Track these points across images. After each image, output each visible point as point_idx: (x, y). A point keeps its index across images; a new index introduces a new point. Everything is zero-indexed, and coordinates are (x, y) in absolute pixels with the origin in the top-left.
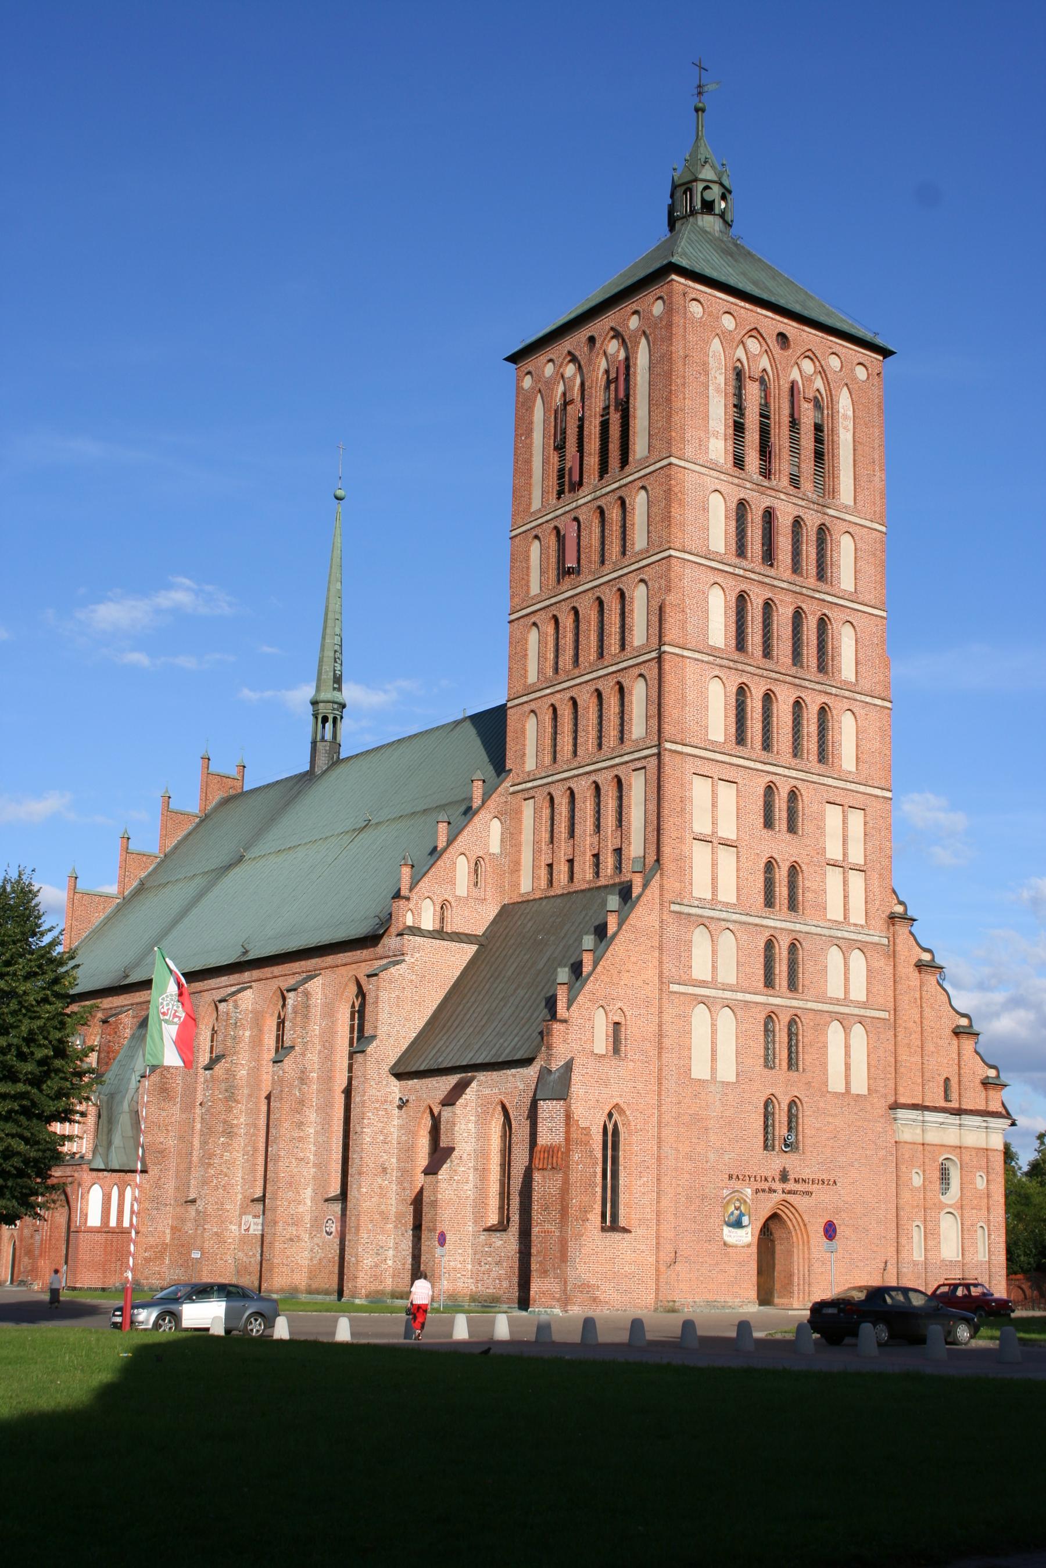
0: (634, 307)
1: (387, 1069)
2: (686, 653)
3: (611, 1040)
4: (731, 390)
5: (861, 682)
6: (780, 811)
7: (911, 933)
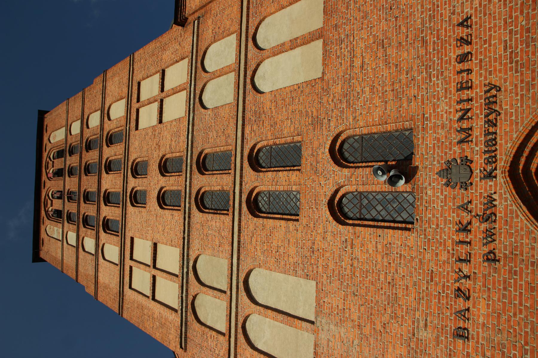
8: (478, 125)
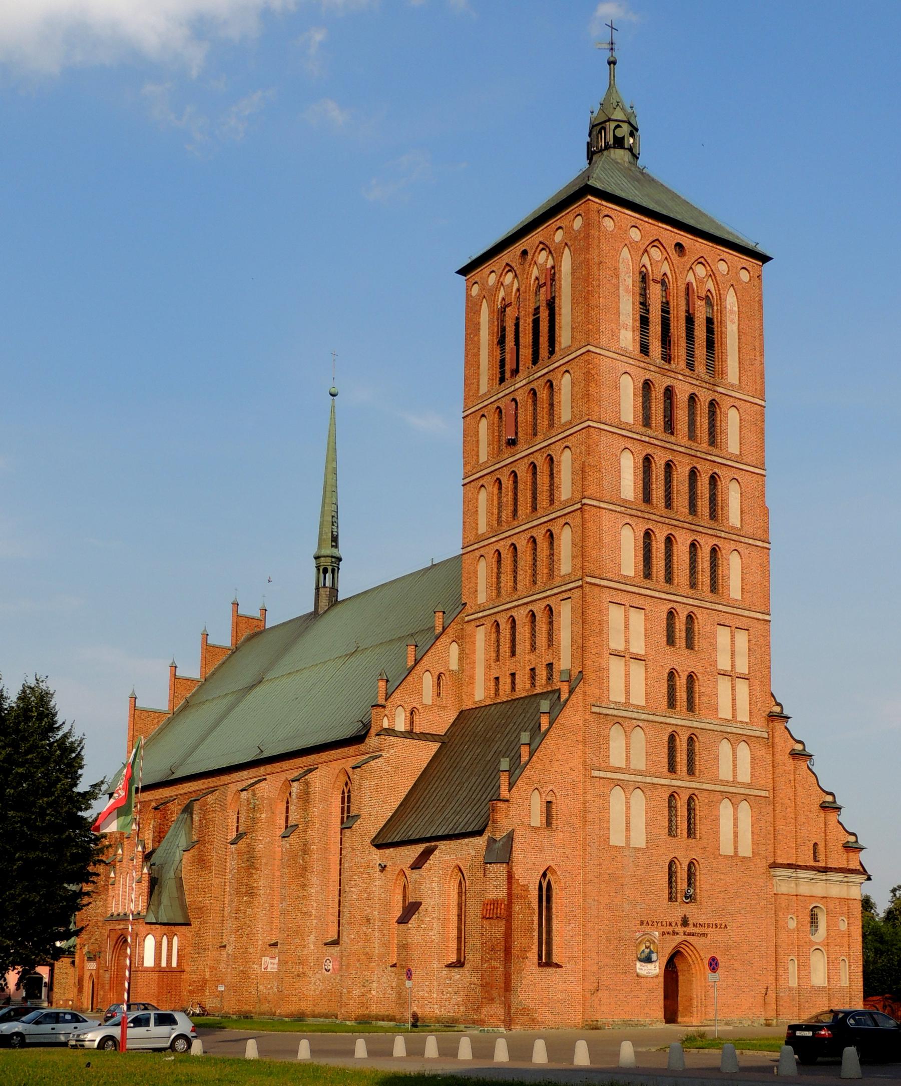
0: (559, 224)
1: (369, 841)
2: (602, 505)
3: (544, 815)
4: (637, 290)
5: (746, 528)
6: (680, 631)
7: (786, 728)
8: (697, 930)
